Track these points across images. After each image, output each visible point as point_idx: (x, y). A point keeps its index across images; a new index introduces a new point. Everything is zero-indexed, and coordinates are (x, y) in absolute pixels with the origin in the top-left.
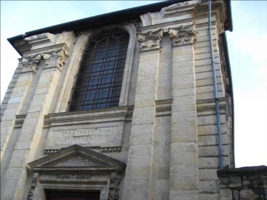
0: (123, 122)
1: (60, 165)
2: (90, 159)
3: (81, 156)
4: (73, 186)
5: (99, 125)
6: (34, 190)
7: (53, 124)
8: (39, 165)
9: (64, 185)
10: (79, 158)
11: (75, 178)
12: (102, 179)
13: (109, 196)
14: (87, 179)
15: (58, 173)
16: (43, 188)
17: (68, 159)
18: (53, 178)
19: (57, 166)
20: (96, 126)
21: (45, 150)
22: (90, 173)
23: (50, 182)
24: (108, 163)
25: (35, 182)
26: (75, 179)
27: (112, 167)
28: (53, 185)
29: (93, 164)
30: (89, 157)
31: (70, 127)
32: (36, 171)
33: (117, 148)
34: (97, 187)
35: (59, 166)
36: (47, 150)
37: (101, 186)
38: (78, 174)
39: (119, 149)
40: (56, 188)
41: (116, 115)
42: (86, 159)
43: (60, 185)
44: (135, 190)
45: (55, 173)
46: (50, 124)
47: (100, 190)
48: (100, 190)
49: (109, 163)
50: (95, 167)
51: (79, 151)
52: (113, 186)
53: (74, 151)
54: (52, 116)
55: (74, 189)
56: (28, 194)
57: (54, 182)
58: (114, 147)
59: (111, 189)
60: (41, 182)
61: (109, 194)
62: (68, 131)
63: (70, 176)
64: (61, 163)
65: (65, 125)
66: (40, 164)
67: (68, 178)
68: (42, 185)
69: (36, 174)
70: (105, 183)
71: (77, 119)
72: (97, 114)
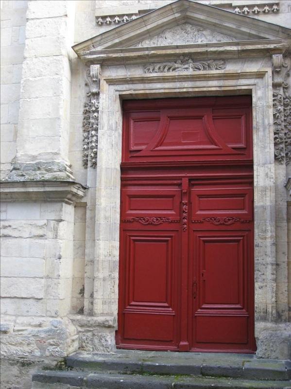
1: (146, 44)
2: (215, 28)
3: (192, 24)
6: (98, 99)
8: (99, 49)
9: (167, 85)
10: (189, 28)
11: (191, 70)
12: (253, 67)
13: (274, 100)
14: (216, 69)
15: (145, 61)
16: (118, 93)
17: (163, 32)
18: (137, 72)
19: (140, 46)
21: (97, 18)
22: (223, 57)
24: (262, 35)
25: (97, 83)
26: (191, 72)
28: (140, 86)
29: (225, 40)
30: (215, 25)
32: (93, 62)
33: (271, 5)
34: (243, 84)
35: (145, 46)
36: (104, 18)
37: (252, 81)
38: (194, 61)
39: (275, 7)
42: (205, 29)
43: (159, 85)
45: (138, 61)
47: (251, 90)
48: (251, 90)
49: (267, 36)
50: (237, 44)
51: (189, 14)
52: (279, 80)
53: (177, 15)
55: (190, 90)
56: (82, 109)
57: (142, 80)
58: (264, 5)
59: (275, 86)
60: (111, 82)
61: (274, 96)
63: (176, 65)
64: (147, 42)
66: (100, 45)
67: (174, 69)
68: (113, 88)
69: (95, 68)
70: (260, 75)
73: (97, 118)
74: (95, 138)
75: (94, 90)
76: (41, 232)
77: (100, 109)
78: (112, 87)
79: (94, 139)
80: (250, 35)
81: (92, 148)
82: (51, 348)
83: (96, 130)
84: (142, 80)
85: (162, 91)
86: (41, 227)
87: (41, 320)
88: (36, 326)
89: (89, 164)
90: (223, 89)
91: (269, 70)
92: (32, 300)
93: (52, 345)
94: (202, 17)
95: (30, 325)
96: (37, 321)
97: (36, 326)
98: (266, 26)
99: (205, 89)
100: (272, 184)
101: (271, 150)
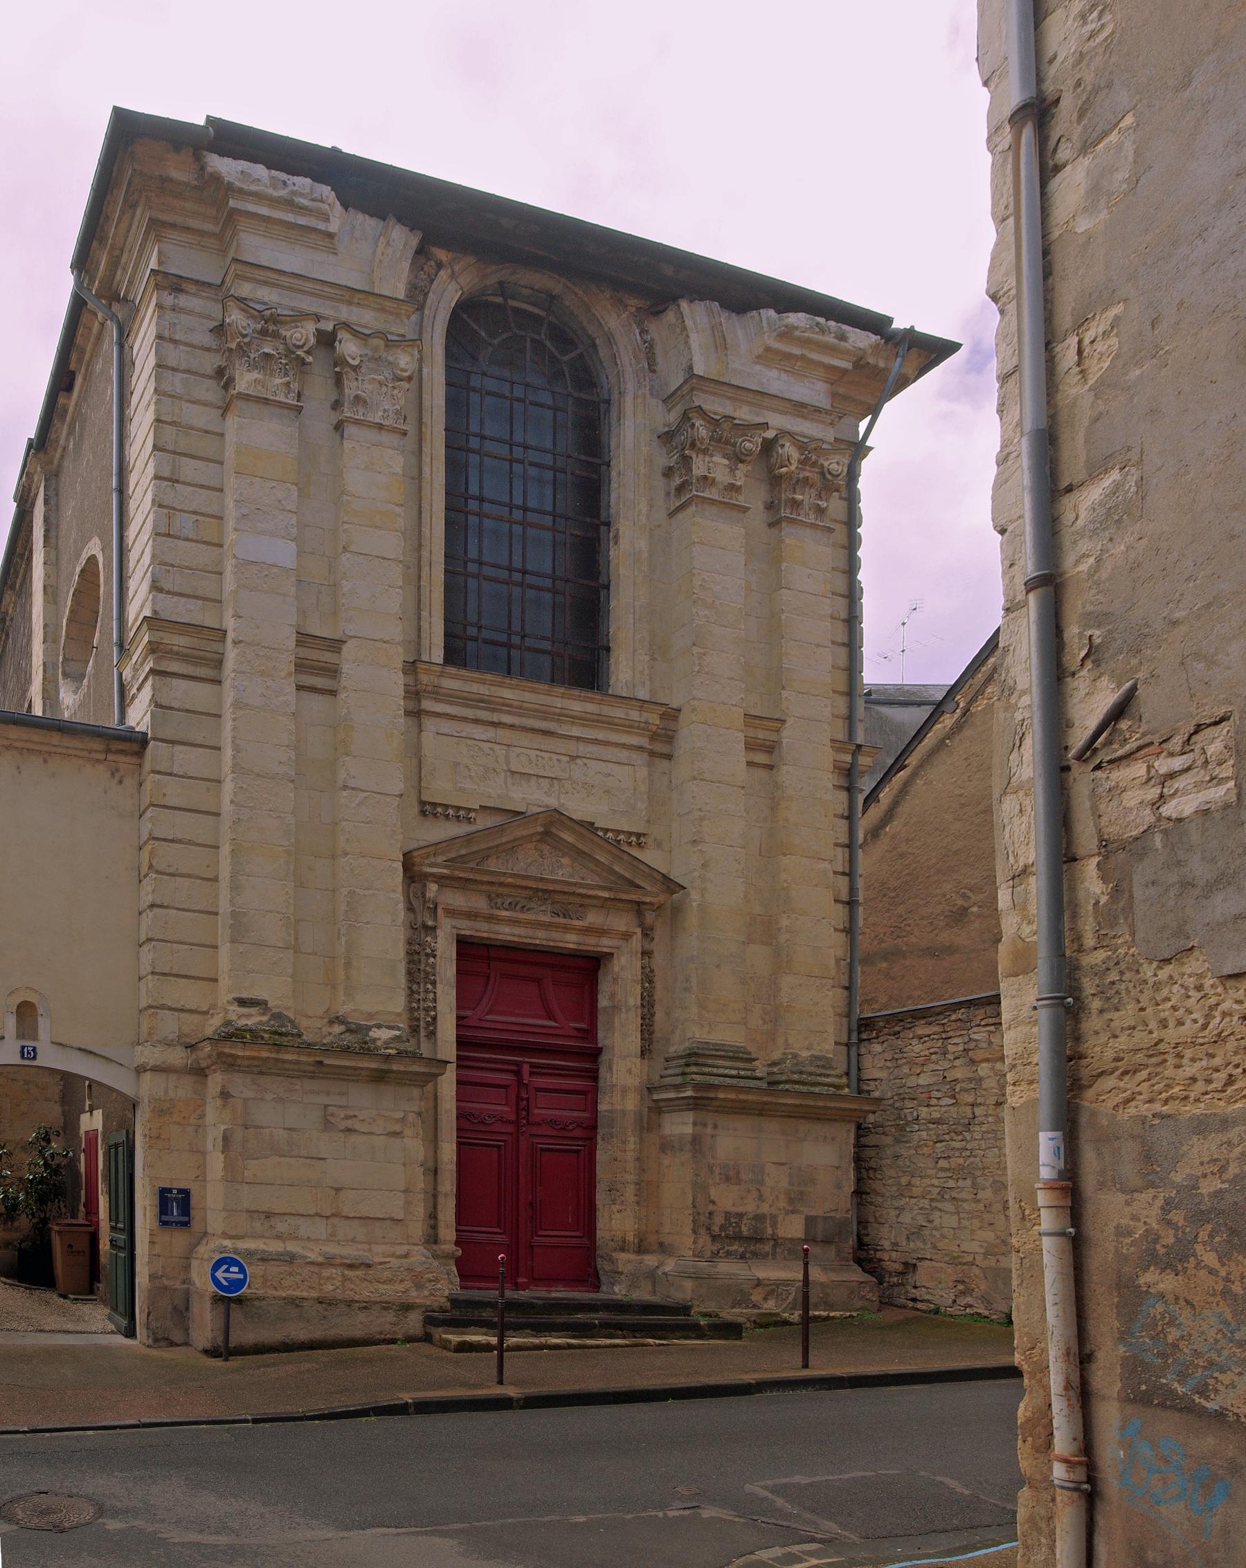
0: (645, 756)
4: (541, 934)
5: (582, 749)
7: (427, 705)
10: (546, 849)
18: (480, 903)
20: (572, 747)
23: (472, 915)
26: (546, 918)
27: (647, 894)
31: (490, 733)
36: (435, 805)
40: (492, 936)
41: (629, 727)
43: (507, 930)
44: (718, 966)
45: (484, 887)
46: (419, 701)
50: (610, 889)
54: (428, 672)
55: (544, 943)
60: (451, 913)
62: (486, 746)
63: (533, 905)
65: (476, 721)
66: (441, 854)
71: (507, 707)
72: (576, 706)
73: (433, 966)
74: (431, 996)
75: (430, 923)
76: (398, 1128)
77: (438, 953)
78: (448, 920)
79: (431, 996)
80: (622, 877)
81: (427, 1010)
82: (430, 1286)
83: (434, 983)
84: (490, 918)
85: (510, 938)
86: (397, 1121)
87: (405, 1248)
88: (400, 1257)
89: (423, 1033)
90: (581, 947)
91: (639, 931)
92: (388, 1222)
93: (430, 1281)
94: (568, 837)
95: (393, 1255)
96: (401, 1250)
97: (400, 1257)
98: (647, 870)
99: (561, 945)
100: (637, 1083)
101: (634, 1041)
